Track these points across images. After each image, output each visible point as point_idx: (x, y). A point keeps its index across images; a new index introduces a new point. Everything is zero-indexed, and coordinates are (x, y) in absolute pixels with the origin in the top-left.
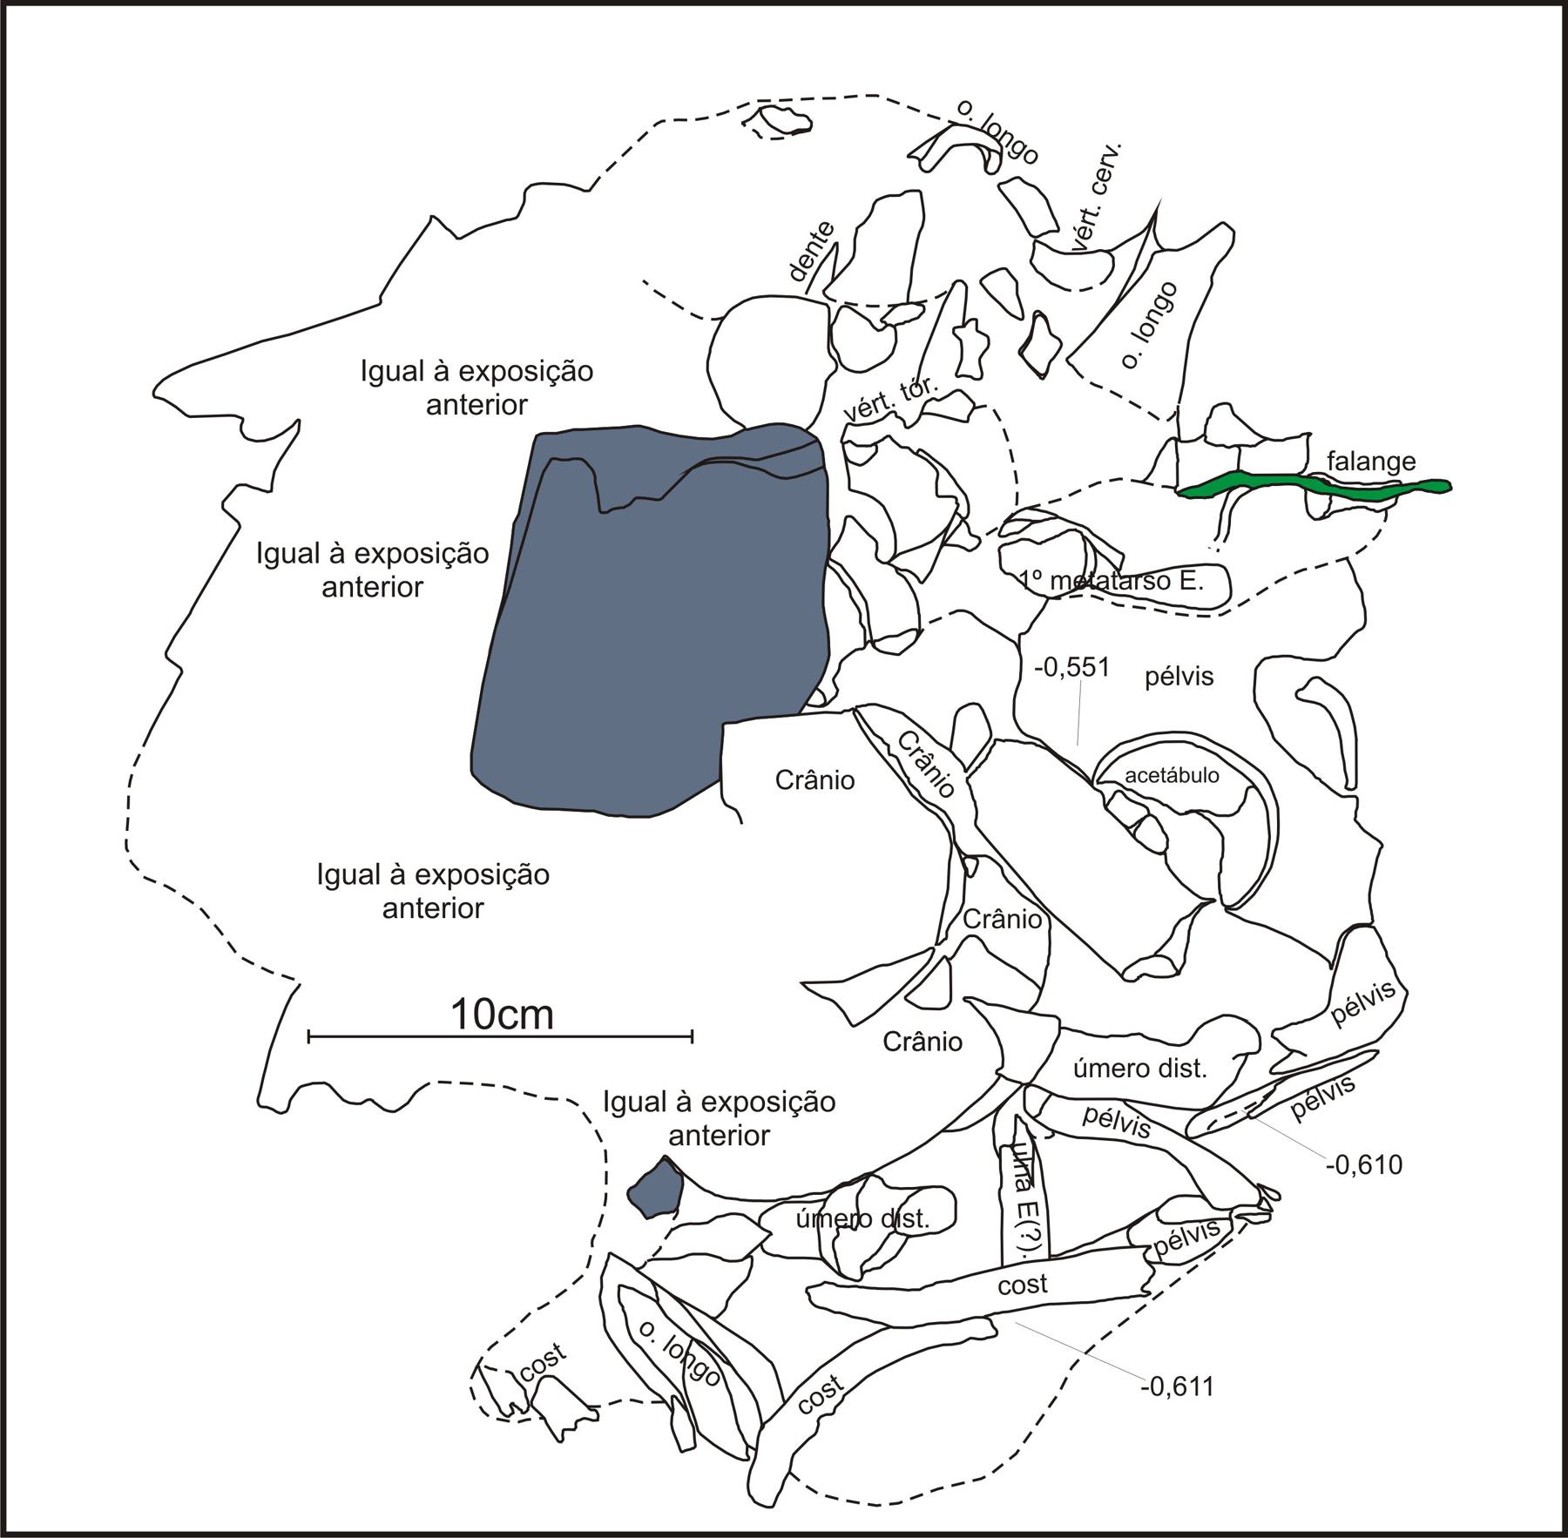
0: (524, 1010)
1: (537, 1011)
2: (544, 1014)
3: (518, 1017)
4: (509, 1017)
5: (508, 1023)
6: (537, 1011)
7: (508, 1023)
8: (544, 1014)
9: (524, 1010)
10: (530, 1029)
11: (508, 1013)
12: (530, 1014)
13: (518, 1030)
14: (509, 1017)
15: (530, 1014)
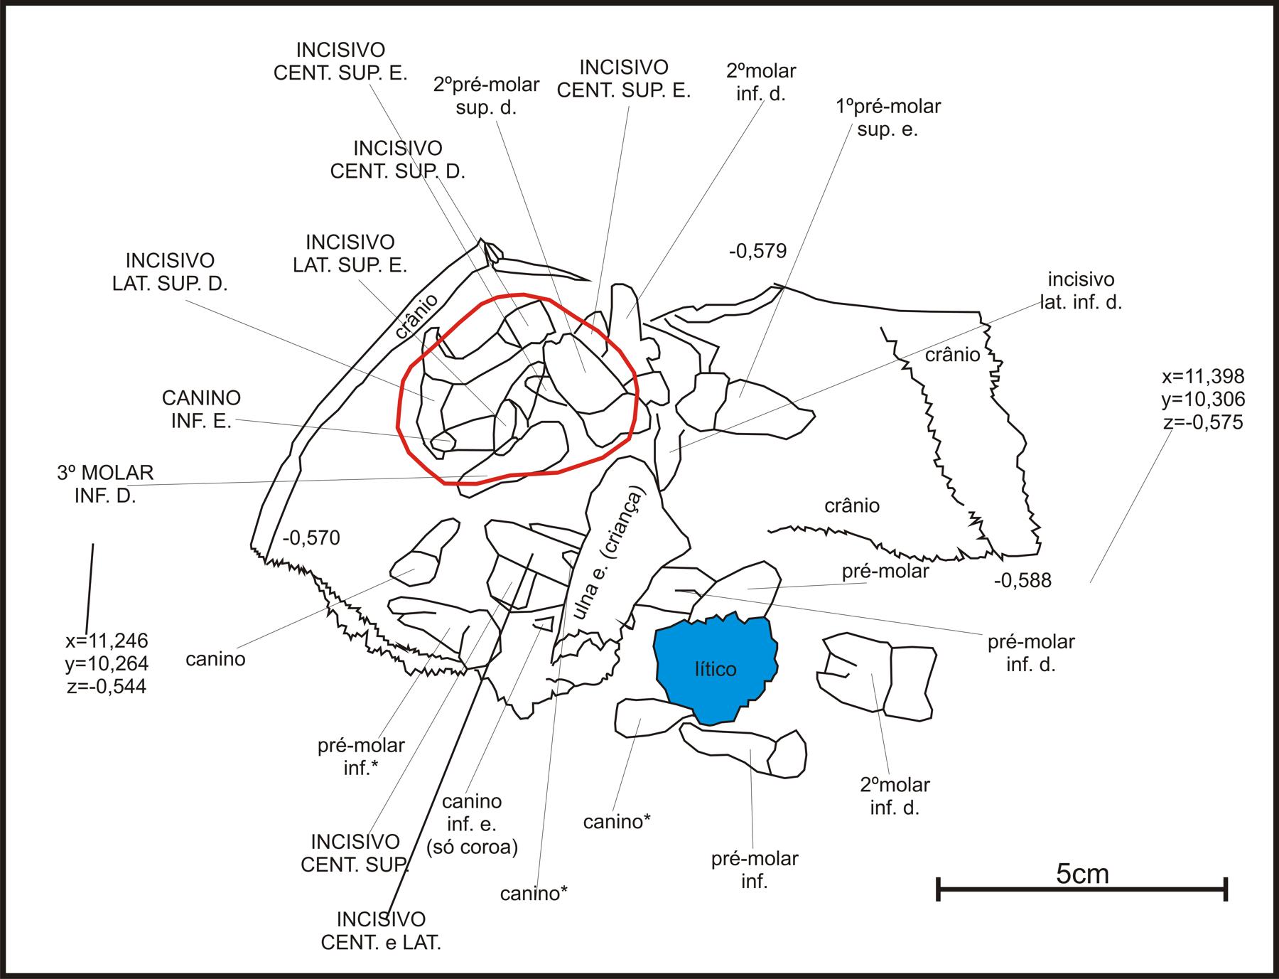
0: (1090, 871)
1: (1098, 872)
2: (1102, 874)
3: (1086, 875)
4: (1080, 876)
5: (1079, 878)
6: (1098, 872)
7: (1079, 878)
8: (1102, 874)
9: (1090, 871)
10: (1094, 884)
11: (1079, 874)
12: (1094, 874)
13: (1085, 885)
14: (1080, 876)
15: (1094, 874)
